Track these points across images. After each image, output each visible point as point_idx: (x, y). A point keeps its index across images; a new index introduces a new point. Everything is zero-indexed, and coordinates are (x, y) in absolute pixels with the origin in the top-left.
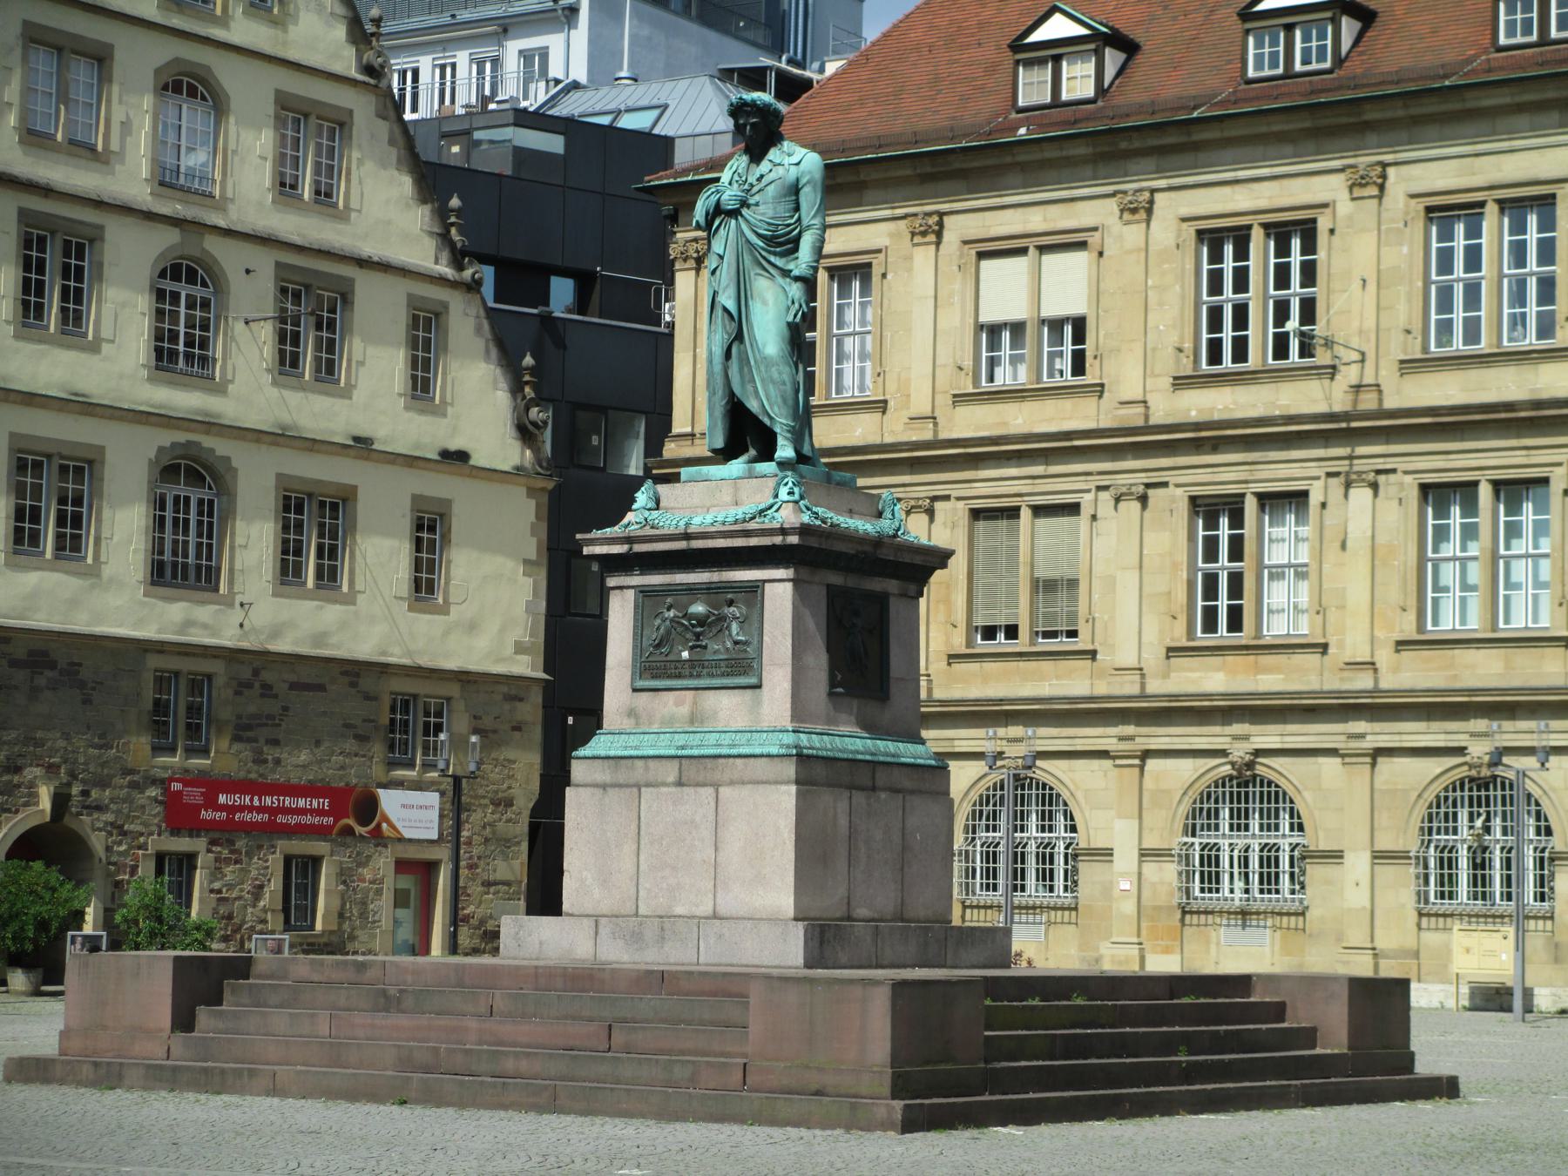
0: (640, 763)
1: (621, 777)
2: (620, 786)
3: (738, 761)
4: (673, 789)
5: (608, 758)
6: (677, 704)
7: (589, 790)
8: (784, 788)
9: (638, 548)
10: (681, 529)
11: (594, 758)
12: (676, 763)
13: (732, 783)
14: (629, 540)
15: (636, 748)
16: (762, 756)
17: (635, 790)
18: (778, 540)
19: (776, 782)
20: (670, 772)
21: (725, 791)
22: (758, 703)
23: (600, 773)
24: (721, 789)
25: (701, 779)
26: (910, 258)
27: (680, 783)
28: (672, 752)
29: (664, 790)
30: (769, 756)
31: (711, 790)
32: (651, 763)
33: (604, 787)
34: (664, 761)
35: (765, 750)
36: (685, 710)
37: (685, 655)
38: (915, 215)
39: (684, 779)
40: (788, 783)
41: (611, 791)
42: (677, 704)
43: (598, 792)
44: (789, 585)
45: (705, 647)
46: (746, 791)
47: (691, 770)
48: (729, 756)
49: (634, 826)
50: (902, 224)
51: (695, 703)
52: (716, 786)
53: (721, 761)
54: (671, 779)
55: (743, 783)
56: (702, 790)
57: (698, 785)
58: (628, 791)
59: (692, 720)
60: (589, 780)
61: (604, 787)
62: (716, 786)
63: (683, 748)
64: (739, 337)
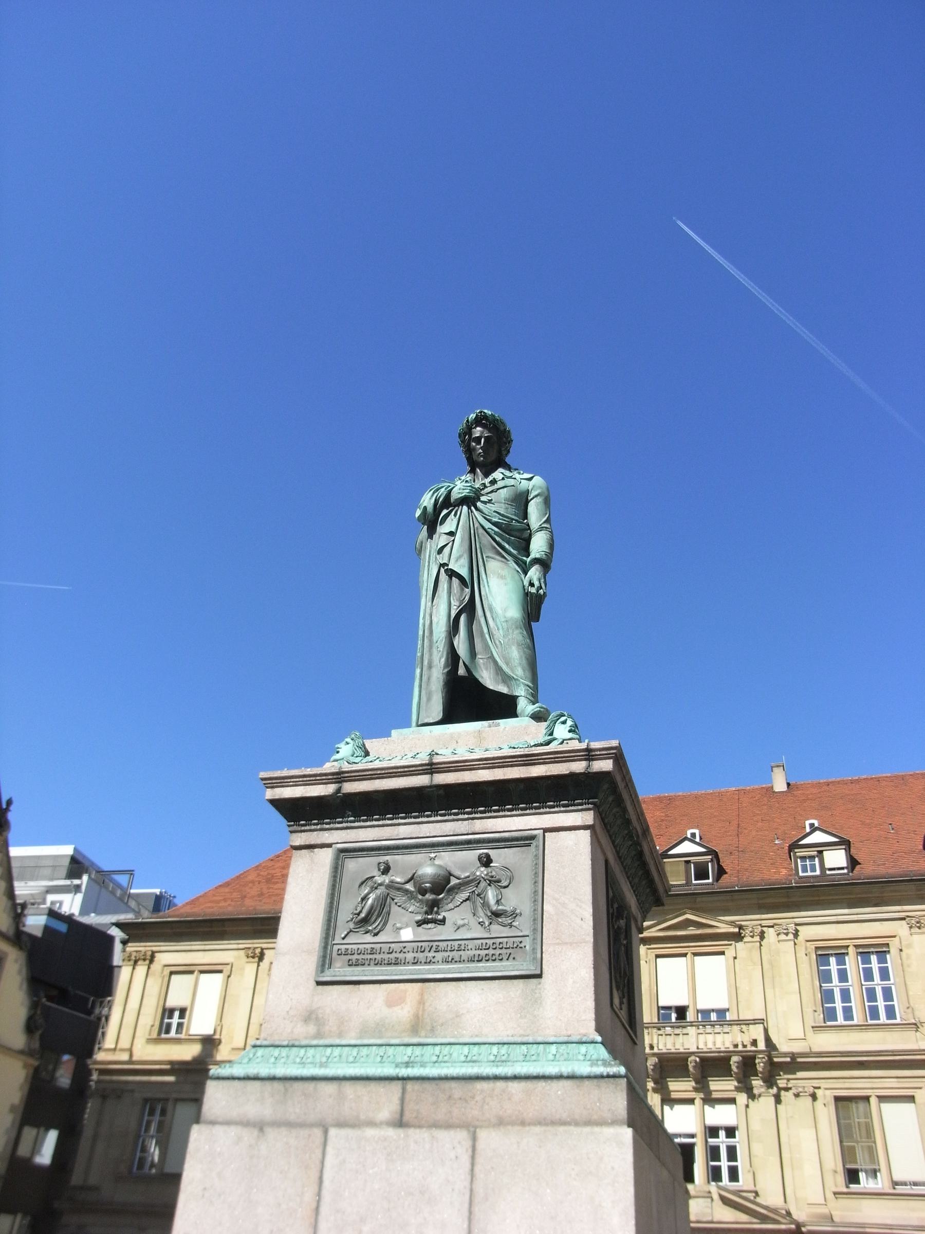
0: (329, 1089)
1: (295, 1109)
2: (290, 1125)
3: (514, 1086)
4: (391, 1132)
5: (273, 1078)
6: (390, 1004)
7: (233, 1131)
8: (609, 1131)
9: (350, 787)
10: (423, 758)
11: (247, 1078)
12: (396, 1087)
13: (501, 1122)
14: (339, 777)
15: (322, 1065)
16: (560, 1077)
17: (318, 1133)
18: (578, 767)
19: (589, 1123)
20: (386, 1101)
21: (488, 1139)
22: (537, 1001)
23: (256, 1103)
24: (482, 1134)
25: (440, 1116)
26: (243, 969)
27: (400, 1123)
28: (390, 1071)
29: (370, 1132)
30: (572, 1077)
31: (462, 1136)
32: (349, 1089)
33: (260, 1126)
34: (373, 1086)
35: (566, 1069)
36: (404, 1013)
37: (407, 934)
38: (249, 948)
39: (408, 1116)
40: (614, 1123)
41: (271, 1133)
42: (390, 1004)
43: (248, 1135)
44: (586, 835)
45: (443, 922)
46: (531, 1137)
47: (422, 1101)
48: (496, 1078)
49: (309, 1196)
50: (242, 952)
51: (421, 1002)
52: (472, 1129)
53: (480, 1085)
54: (386, 1112)
55: (523, 1123)
56: (444, 1136)
57: (436, 1125)
58: (304, 1132)
59: (416, 1026)
60: (234, 1114)
61: (260, 1126)
62: (472, 1129)
63: (407, 1064)
64: (469, 609)
